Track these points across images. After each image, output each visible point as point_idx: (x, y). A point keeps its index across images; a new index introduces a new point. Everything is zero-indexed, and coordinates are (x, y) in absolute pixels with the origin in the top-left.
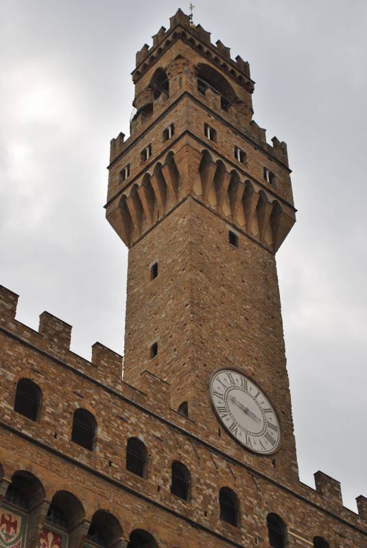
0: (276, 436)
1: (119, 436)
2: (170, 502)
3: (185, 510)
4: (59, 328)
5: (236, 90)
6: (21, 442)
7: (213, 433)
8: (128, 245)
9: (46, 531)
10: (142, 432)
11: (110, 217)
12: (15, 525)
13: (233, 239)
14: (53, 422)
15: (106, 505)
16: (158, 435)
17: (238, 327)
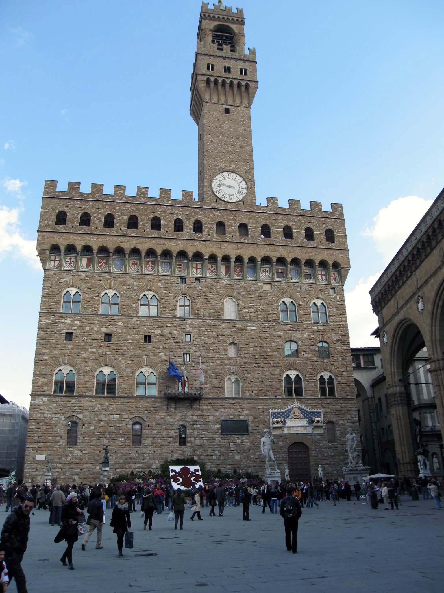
0: (245, 191)
1: (170, 221)
2: (193, 236)
3: (200, 237)
4: (143, 190)
5: (235, 29)
6: (131, 238)
7: (212, 202)
8: (198, 123)
9: (149, 262)
10: (180, 215)
11: (191, 115)
12: (137, 264)
13: (227, 111)
14: (143, 226)
15: (165, 248)
16: (187, 213)
17: (227, 151)
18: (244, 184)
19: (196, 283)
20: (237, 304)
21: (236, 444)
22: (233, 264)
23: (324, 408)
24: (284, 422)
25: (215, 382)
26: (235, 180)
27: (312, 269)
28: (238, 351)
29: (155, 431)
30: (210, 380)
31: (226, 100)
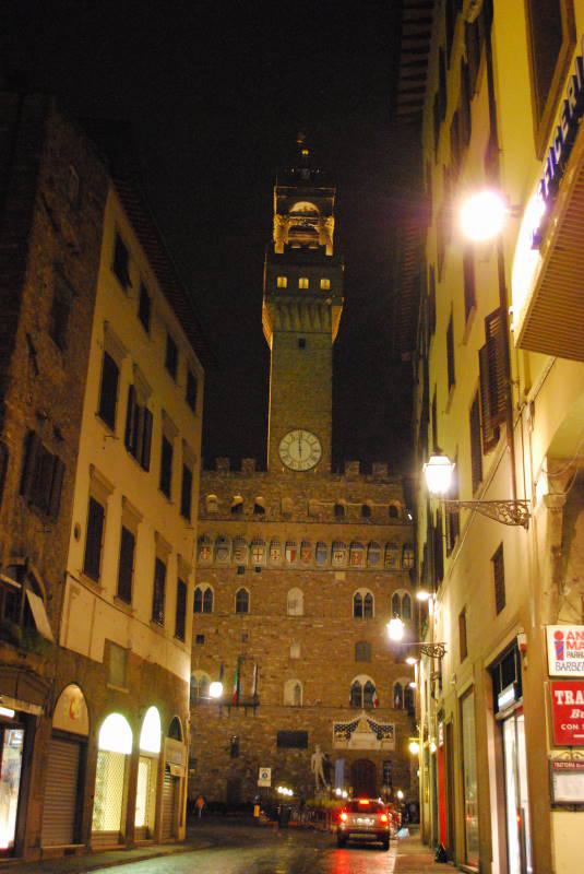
0: (318, 455)
13: (302, 344)
18: (318, 446)
19: (254, 573)
20: (304, 597)
21: (295, 760)
22: (299, 551)
23: (396, 720)
24: (348, 737)
25: (273, 686)
26: (307, 441)
27: (397, 551)
28: (302, 652)
29: (205, 742)
30: (266, 685)
31: (302, 326)
